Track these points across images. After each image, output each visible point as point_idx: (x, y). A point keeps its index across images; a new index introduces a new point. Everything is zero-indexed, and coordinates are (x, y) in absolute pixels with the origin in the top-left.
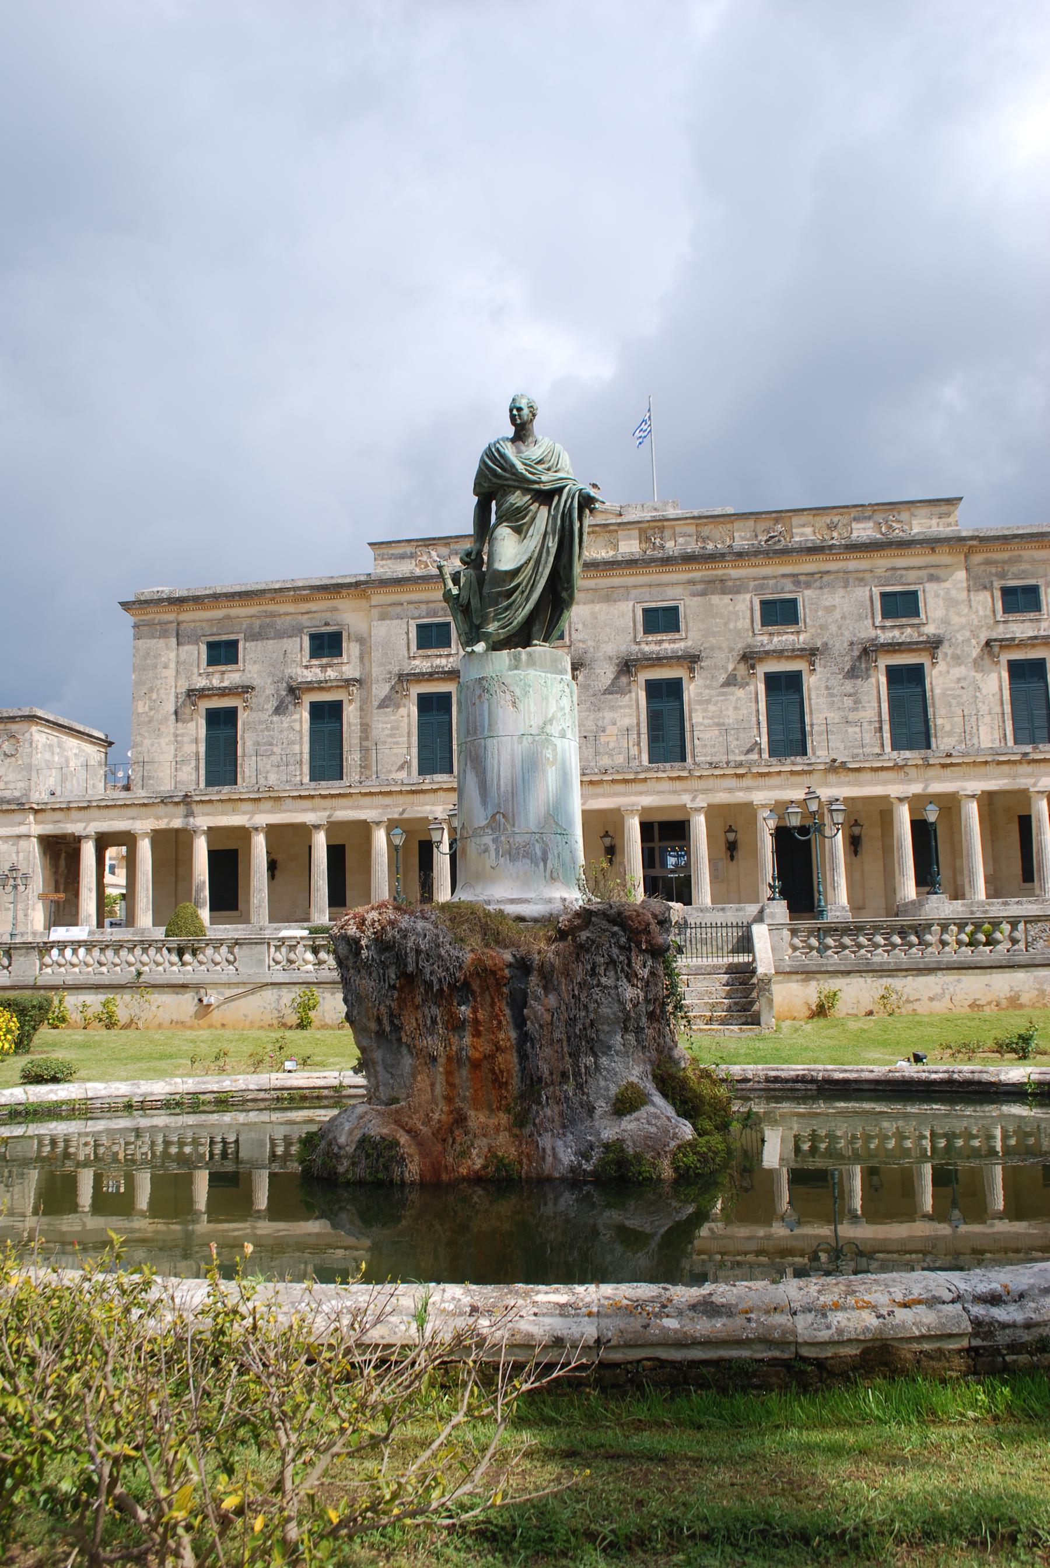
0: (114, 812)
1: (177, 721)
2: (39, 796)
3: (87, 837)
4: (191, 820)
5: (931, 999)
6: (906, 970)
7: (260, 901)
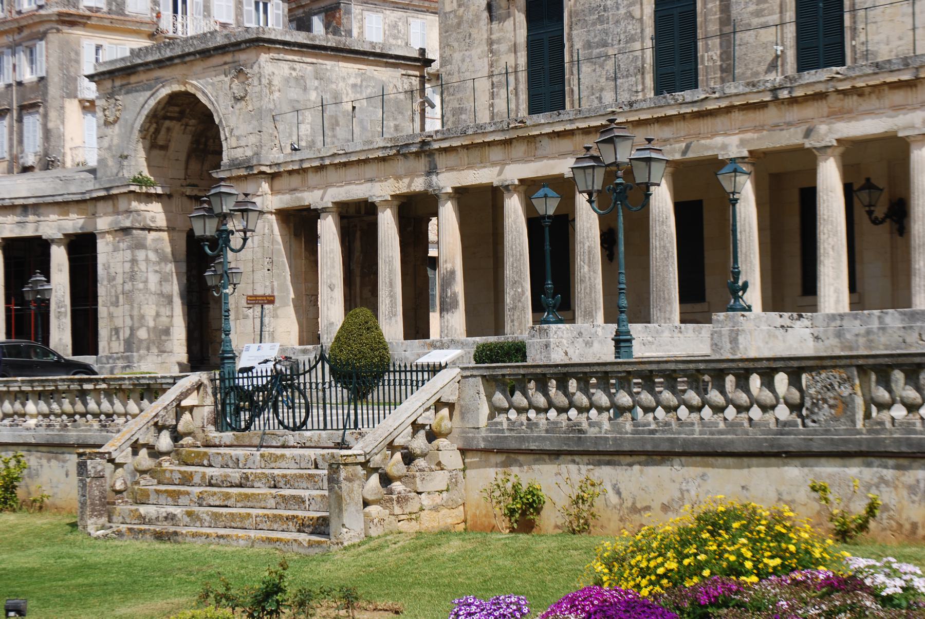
0: (352, 172)
1: (491, 19)
2: (273, 156)
3: (324, 210)
4: (434, 177)
5: (665, 508)
6: (631, 453)
7: (518, 298)
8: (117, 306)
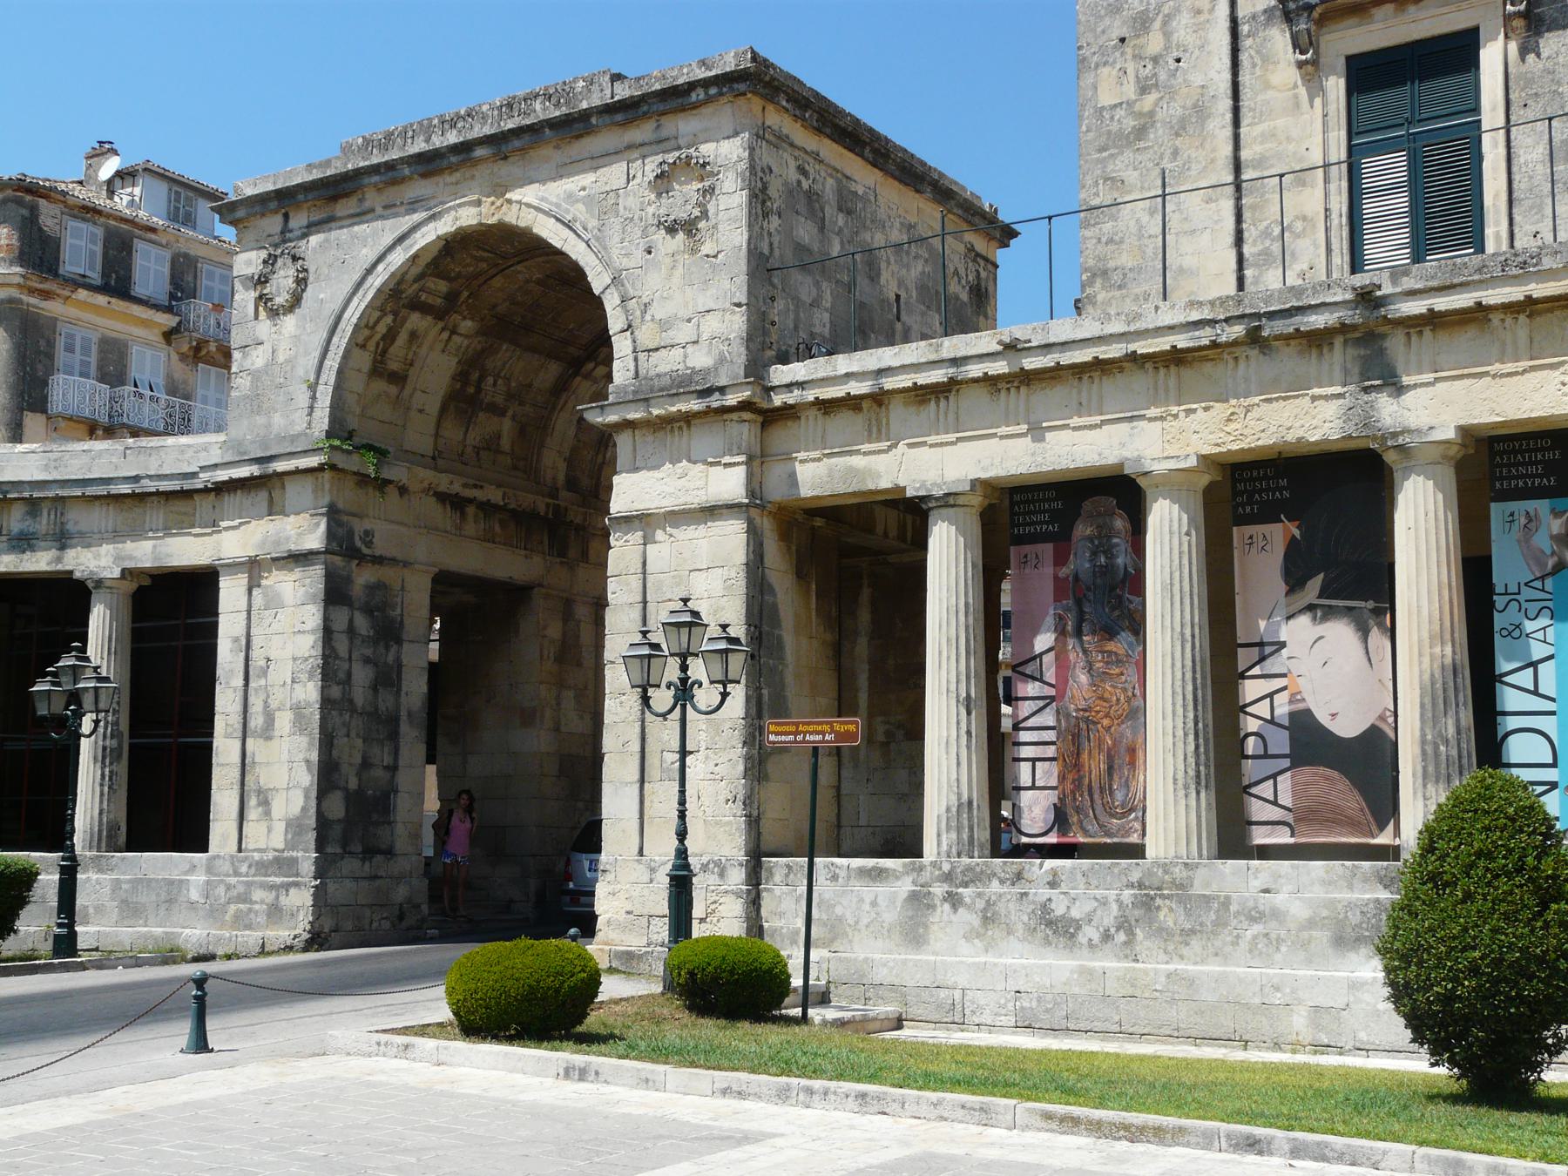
8: (269, 738)
